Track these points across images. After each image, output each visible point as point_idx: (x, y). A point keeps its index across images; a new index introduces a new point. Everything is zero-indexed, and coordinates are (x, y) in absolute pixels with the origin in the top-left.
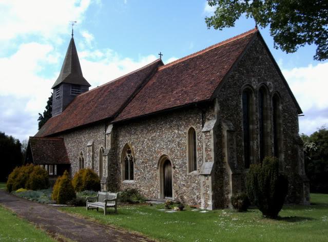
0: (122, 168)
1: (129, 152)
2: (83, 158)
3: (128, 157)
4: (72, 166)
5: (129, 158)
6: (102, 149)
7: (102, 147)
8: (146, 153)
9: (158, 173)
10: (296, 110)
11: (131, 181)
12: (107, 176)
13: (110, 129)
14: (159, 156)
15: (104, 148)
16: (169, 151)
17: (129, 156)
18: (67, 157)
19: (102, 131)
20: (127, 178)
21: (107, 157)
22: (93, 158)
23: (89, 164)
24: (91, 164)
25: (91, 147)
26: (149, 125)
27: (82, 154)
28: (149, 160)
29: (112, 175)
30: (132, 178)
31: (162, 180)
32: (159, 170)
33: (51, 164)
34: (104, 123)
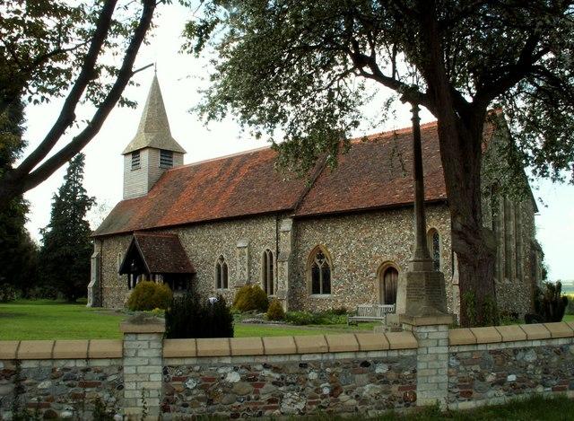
0: (309, 279)
1: (321, 256)
2: (225, 266)
3: (318, 264)
4: (198, 276)
5: (320, 266)
6: (268, 253)
7: (268, 250)
8: (353, 258)
9: (377, 284)
10: (531, 208)
11: (327, 295)
12: (287, 289)
13: (287, 225)
14: (378, 262)
15: (274, 251)
16: (395, 257)
17: (321, 262)
18: (188, 263)
19: (268, 226)
20: (316, 290)
21: (287, 263)
22: (249, 265)
23: (242, 273)
24: (246, 273)
25: (246, 250)
26: (360, 223)
27: (222, 259)
28: (361, 267)
29: (293, 288)
30: (327, 290)
31: (383, 292)
32: (377, 280)
33: (158, 274)
34: (279, 215)
